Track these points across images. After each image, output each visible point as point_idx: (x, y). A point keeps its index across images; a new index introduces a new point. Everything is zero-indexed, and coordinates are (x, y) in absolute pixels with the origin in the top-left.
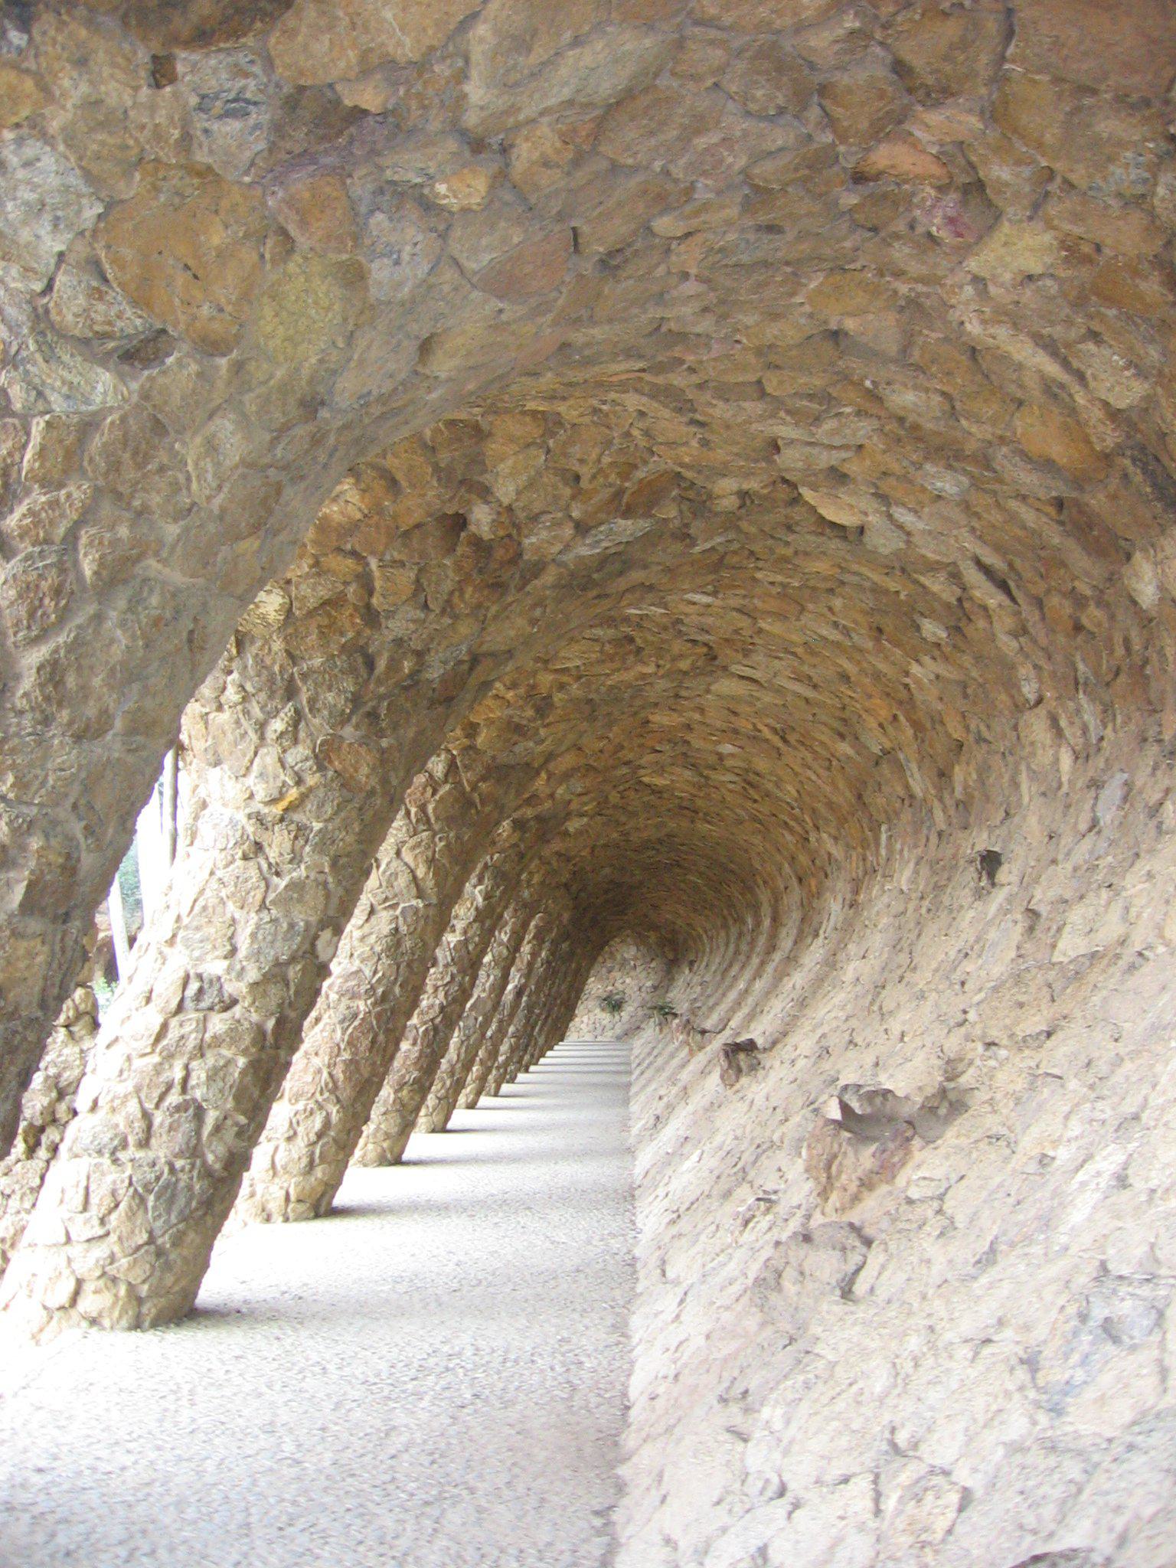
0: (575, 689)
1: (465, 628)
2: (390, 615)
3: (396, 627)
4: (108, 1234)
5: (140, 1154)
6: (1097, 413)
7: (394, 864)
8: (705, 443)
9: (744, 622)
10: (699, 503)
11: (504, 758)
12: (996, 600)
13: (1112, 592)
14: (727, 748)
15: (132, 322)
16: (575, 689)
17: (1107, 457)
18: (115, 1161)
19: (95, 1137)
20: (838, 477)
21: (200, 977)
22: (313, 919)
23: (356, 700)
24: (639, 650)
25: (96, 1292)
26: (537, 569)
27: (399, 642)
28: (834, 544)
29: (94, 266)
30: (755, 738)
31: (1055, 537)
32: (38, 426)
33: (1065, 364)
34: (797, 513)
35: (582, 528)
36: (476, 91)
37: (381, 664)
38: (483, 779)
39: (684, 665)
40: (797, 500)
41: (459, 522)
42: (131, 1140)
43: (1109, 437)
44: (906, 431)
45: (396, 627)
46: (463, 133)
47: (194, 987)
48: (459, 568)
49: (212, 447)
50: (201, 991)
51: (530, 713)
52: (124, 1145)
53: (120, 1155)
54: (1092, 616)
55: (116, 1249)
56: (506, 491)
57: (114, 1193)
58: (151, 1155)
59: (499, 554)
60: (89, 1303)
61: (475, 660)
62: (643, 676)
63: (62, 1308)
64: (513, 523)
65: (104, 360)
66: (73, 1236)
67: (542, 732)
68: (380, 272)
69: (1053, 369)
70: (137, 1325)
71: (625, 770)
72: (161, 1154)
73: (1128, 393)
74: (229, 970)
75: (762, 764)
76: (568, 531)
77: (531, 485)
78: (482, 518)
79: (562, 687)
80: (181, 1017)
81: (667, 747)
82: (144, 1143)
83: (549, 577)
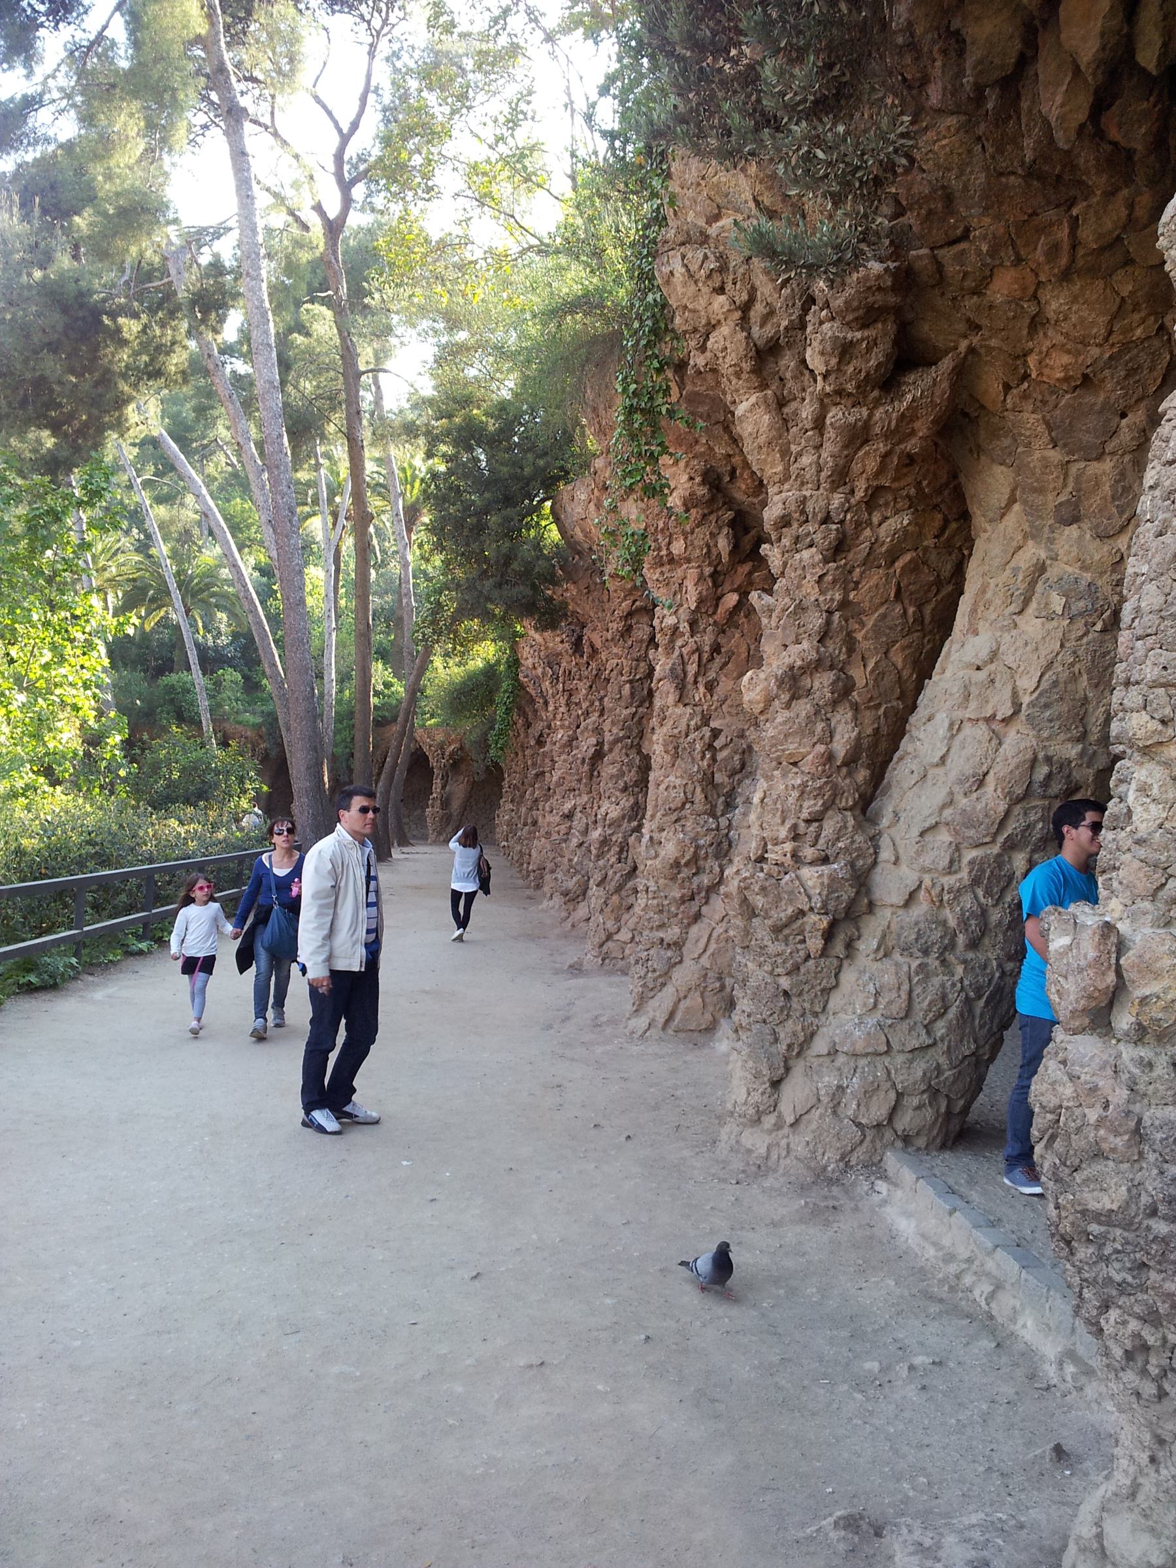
4: (935, 1044)
5: (970, 955)
7: (883, 663)
18: (944, 962)
19: (919, 936)
21: (1049, 760)
25: (918, 1108)
42: (961, 939)
47: (1042, 771)
50: (1049, 776)
52: (952, 946)
53: (951, 958)
55: (943, 1060)
57: (944, 997)
58: (982, 957)
60: (905, 1121)
63: (879, 1126)
66: (895, 1046)
70: (943, 1147)
72: (992, 955)
74: (1081, 755)
80: (1024, 804)
82: (973, 945)
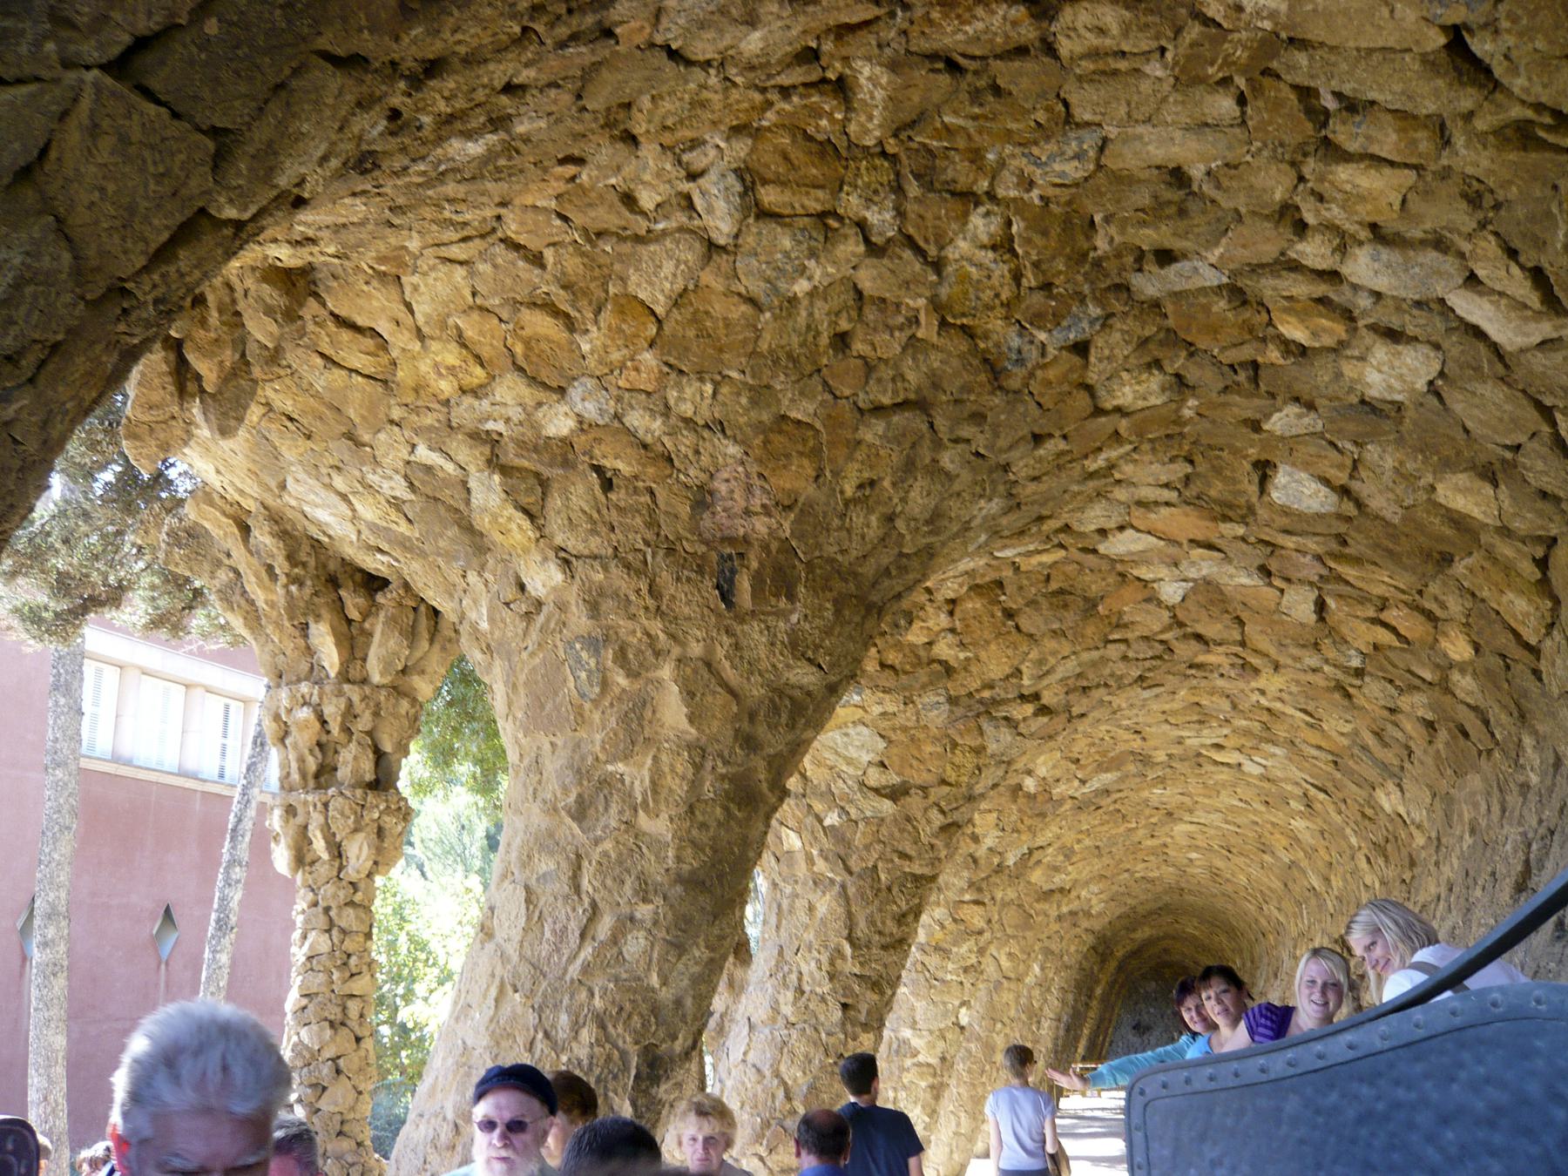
0: (1087, 842)
1: (1024, 837)
2: (985, 836)
3: (989, 842)
6: (1334, 734)
8: (1144, 739)
9: (1186, 799)
10: (1145, 760)
11: (1046, 887)
12: (1322, 796)
13: (1371, 802)
14: (1194, 855)
15: (895, 779)
16: (1087, 842)
17: (1349, 748)
20: (1218, 747)
22: (957, 1003)
23: (971, 884)
24: (1124, 817)
26: (1061, 802)
27: (990, 849)
28: (1225, 769)
29: (882, 764)
30: (1210, 849)
31: (1338, 775)
32: (861, 825)
33: (1311, 716)
34: (1201, 760)
35: (1083, 782)
36: (1026, 682)
37: (982, 862)
38: (1038, 901)
39: (1153, 820)
40: (1199, 755)
41: (1019, 787)
43: (1345, 742)
44: (1247, 733)
45: (989, 842)
46: (1022, 697)
47: (895, 1046)
48: (1020, 810)
49: (929, 822)
51: (1061, 858)
54: (1369, 812)
56: (1042, 771)
59: (1040, 798)
61: (1031, 852)
62: (1130, 830)
64: (1045, 786)
65: (885, 796)
67: (1070, 868)
68: (992, 747)
69: (1308, 718)
71: (1126, 875)
73: (1347, 728)
75: (1219, 863)
76: (1076, 783)
77: (1054, 767)
78: (1030, 784)
79: (1079, 841)
81: (1152, 858)
83: (1068, 805)
